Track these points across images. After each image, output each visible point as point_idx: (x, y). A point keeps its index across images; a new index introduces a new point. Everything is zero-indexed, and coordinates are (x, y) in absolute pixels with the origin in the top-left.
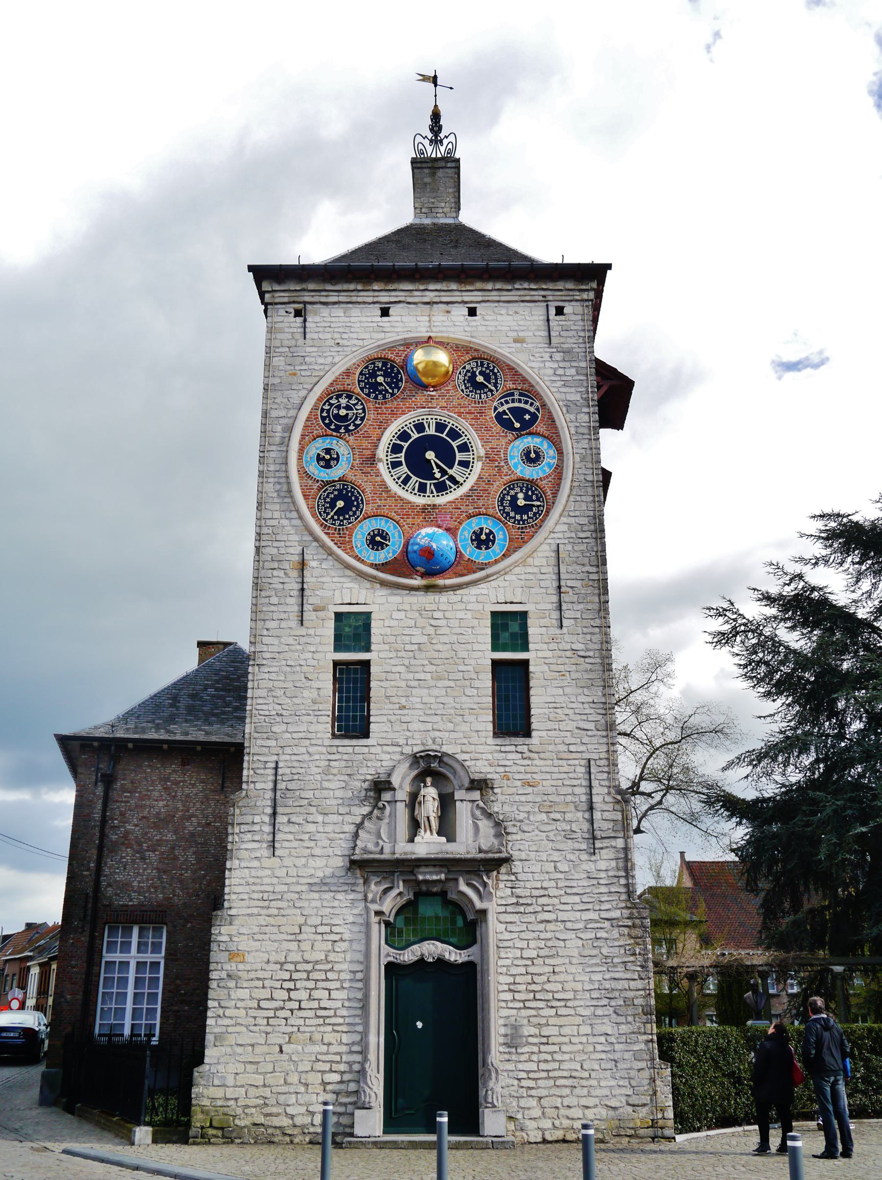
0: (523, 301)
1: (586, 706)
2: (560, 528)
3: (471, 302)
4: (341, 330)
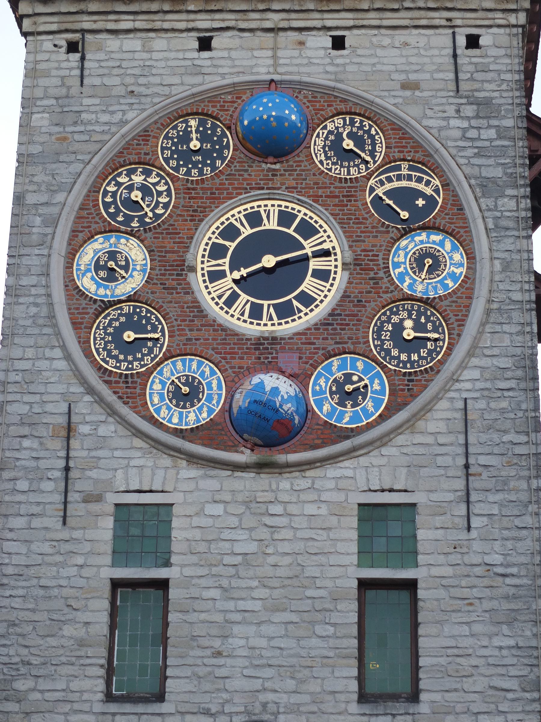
0: (416, 27)
1: (505, 652)
2: (467, 374)
3: (337, 28)
4: (137, 71)
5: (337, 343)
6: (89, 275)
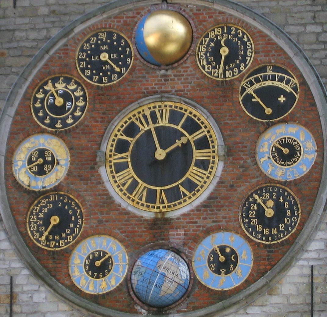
5: (214, 222)
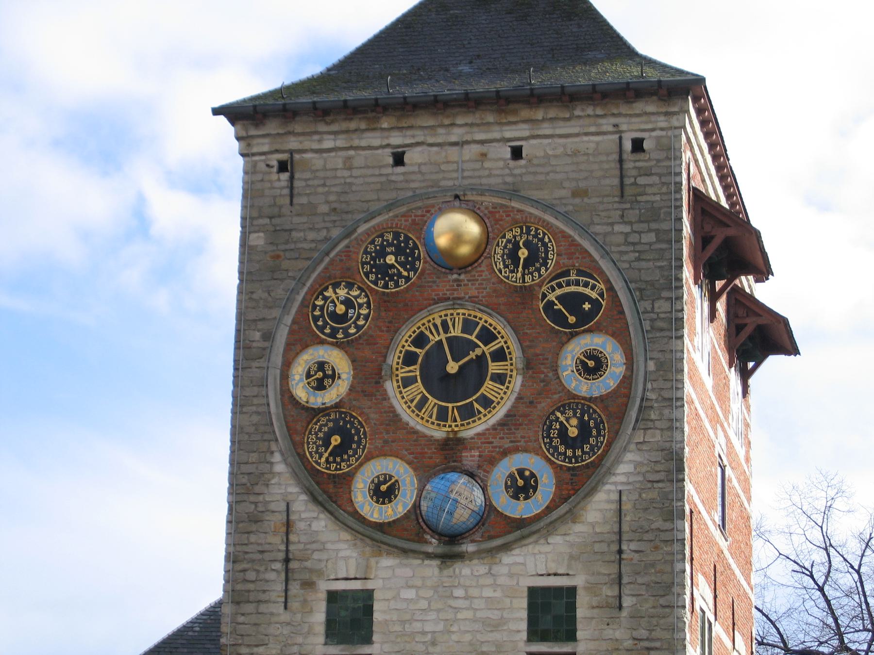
5: (511, 442)
6: (301, 385)
